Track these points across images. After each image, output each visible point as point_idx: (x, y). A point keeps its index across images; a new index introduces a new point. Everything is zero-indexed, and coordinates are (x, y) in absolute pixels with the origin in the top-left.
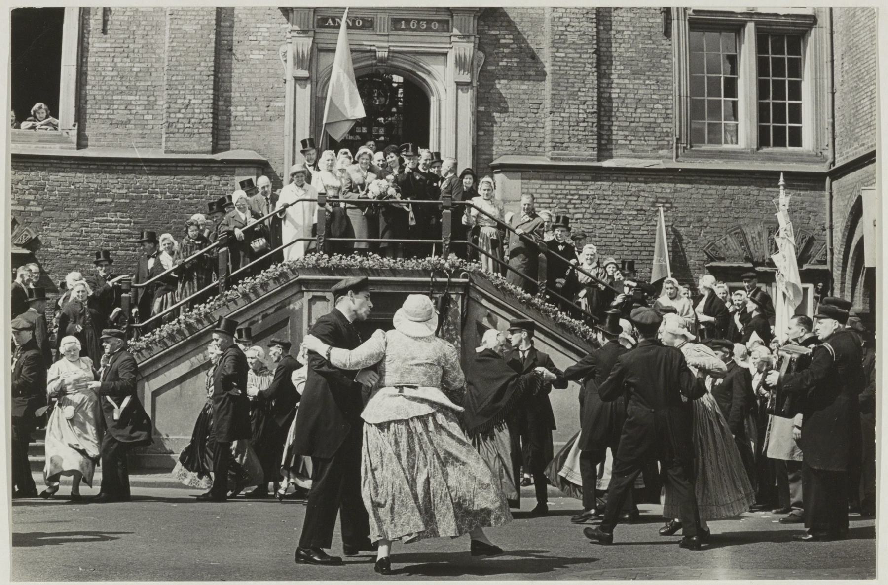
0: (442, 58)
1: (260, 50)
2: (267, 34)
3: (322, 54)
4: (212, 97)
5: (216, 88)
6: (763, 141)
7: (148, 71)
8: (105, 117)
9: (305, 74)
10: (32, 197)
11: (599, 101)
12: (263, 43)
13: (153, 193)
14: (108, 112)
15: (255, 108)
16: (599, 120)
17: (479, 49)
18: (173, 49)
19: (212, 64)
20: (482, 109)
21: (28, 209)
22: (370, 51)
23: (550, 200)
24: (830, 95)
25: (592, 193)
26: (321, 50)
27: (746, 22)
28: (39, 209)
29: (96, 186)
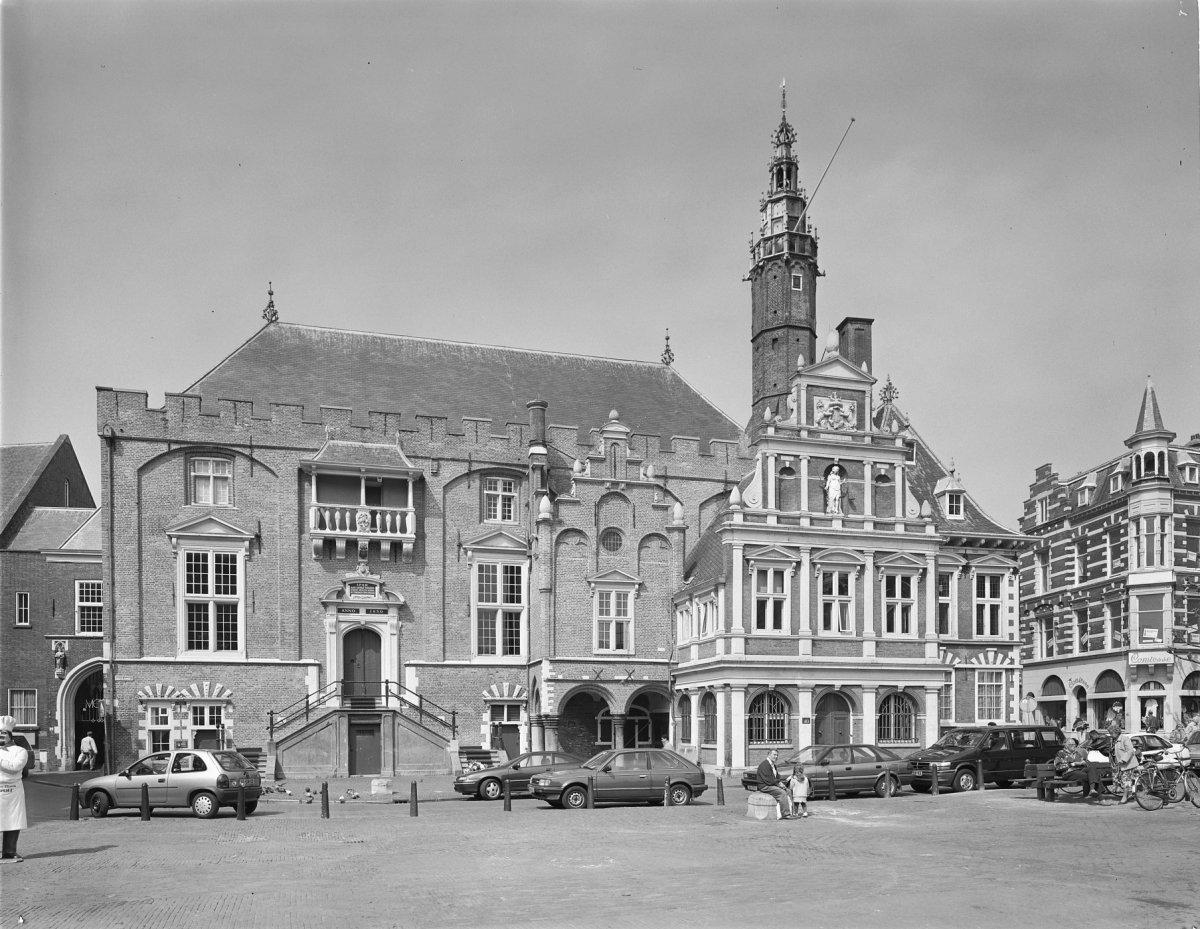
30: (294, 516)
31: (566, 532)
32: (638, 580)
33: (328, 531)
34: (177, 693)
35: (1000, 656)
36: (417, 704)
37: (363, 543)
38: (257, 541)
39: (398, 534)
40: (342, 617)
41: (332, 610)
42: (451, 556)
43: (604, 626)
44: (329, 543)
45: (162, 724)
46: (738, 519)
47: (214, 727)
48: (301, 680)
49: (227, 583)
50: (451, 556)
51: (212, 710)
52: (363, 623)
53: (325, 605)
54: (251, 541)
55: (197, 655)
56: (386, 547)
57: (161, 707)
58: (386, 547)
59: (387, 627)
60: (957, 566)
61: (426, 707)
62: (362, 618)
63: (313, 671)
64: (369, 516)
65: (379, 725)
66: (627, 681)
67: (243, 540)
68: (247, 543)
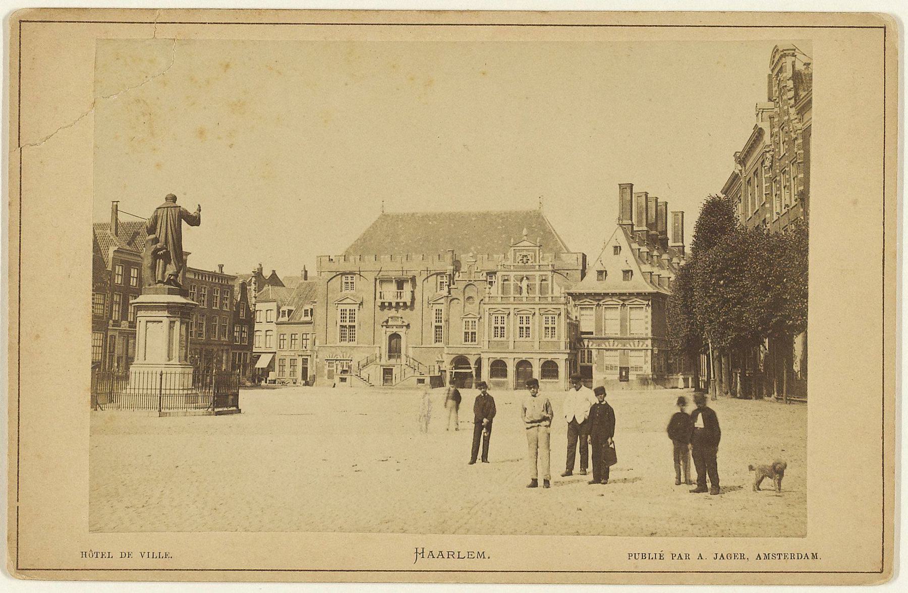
31: (453, 299)
32: (479, 316)
33: (382, 300)
34: (336, 357)
35: (641, 343)
37: (394, 304)
38: (361, 304)
40: (388, 329)
41: (384, 327)
42: (425, 305)
43: (466, 333)
44: (383, 303)
46: (487, 300)
47: (347, 369)
49: (352, 319)
50: (425, 305)
52: (394, 332)
53: (382, 326)
54: (360, 304)
55: (343, 344)
56: (401, 304)
58: (401, 304)
59: (402, 332)
60: (619, 305)
62: (395, 330)
64: (396, 293)
66: (474, 355)
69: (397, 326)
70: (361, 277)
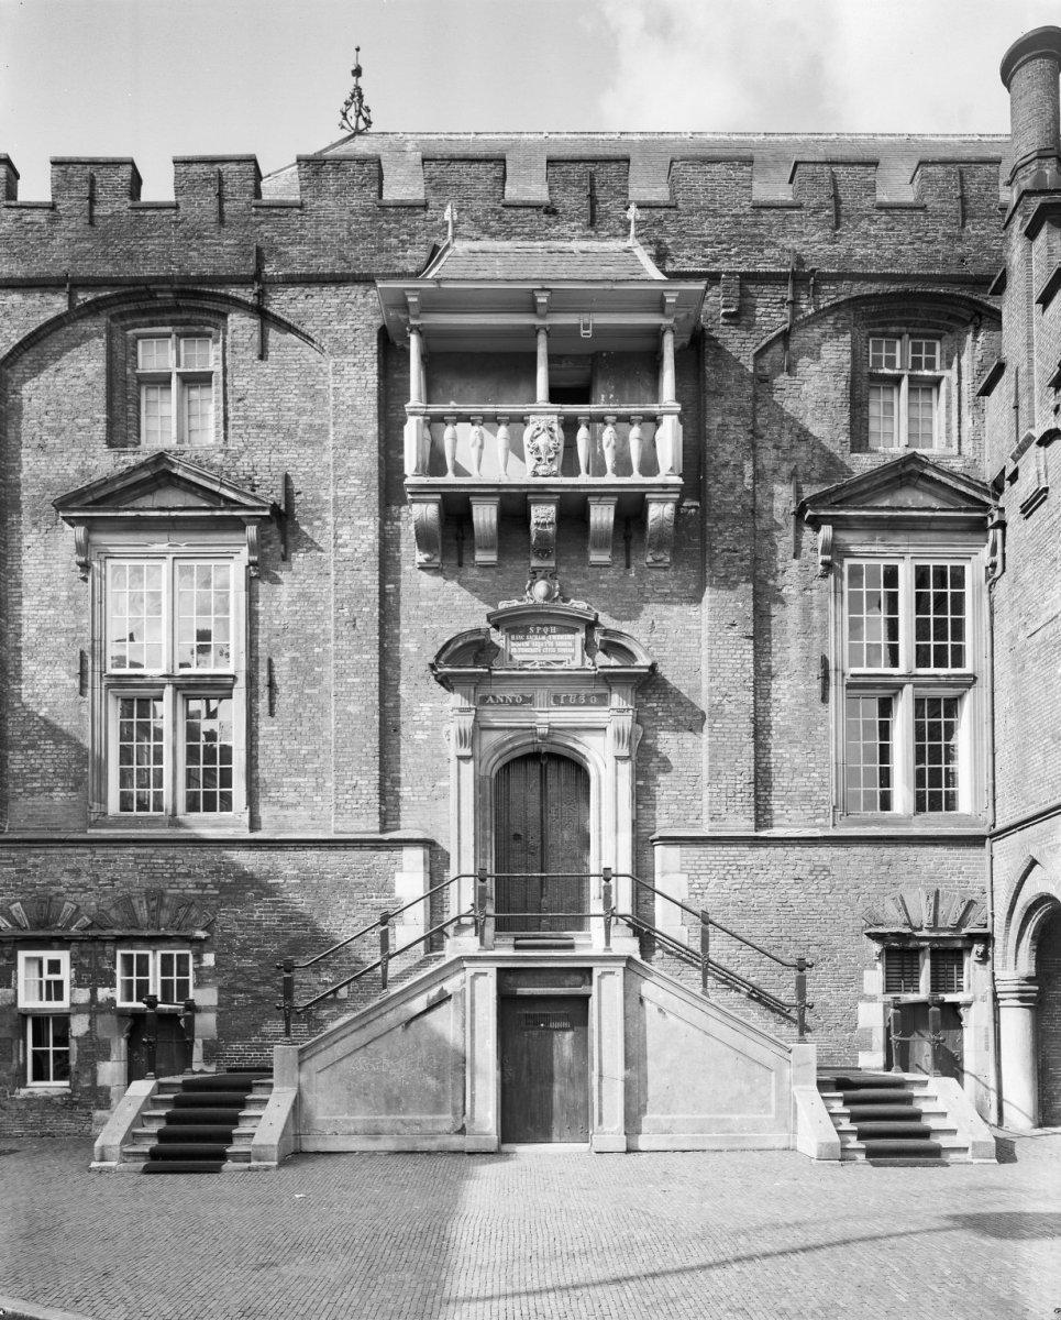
0: (602, 733)
1: (423, 730)
2: (430, 714)
3: (484, 733)
4: (378, 777)
5: (382, 768)
6: (920, 807)
7: (316, 753)
8: (275, 800)
9: (467, 752)
10: (209, 881)
11: (755, 771)
12: (426, 723)
13: (323, 873)
14: (278, 794)
15: (421, 788)
16: (756, 791)
17: (637, 723)
18: (338, 731)
19: (377, 745)
20: (641, 783)
21: (205, 892)
22: (531, 728)
23: (708, 872)
24: (990, 757)
25: (750, 863)
26: (483, 729)
27: (904, 684)
28: (217, 892)
29: (268, 868)
30: (365, 458)
36: (696, 946)
37: (542, 514)
39: (636, 478)
44: (456, 509)
45: (56, 999)
48: (386, 887)
51: (166, 960)
54: (262, 522)
56: (602, 516)
57: (48, 955)
61: (720, 948)
63: (414, 858)
64: (559, 434)
65: (585, 999)
67: (238, 525)
68: (252, 531)
69: (568, 688)
70: (274, 336)
